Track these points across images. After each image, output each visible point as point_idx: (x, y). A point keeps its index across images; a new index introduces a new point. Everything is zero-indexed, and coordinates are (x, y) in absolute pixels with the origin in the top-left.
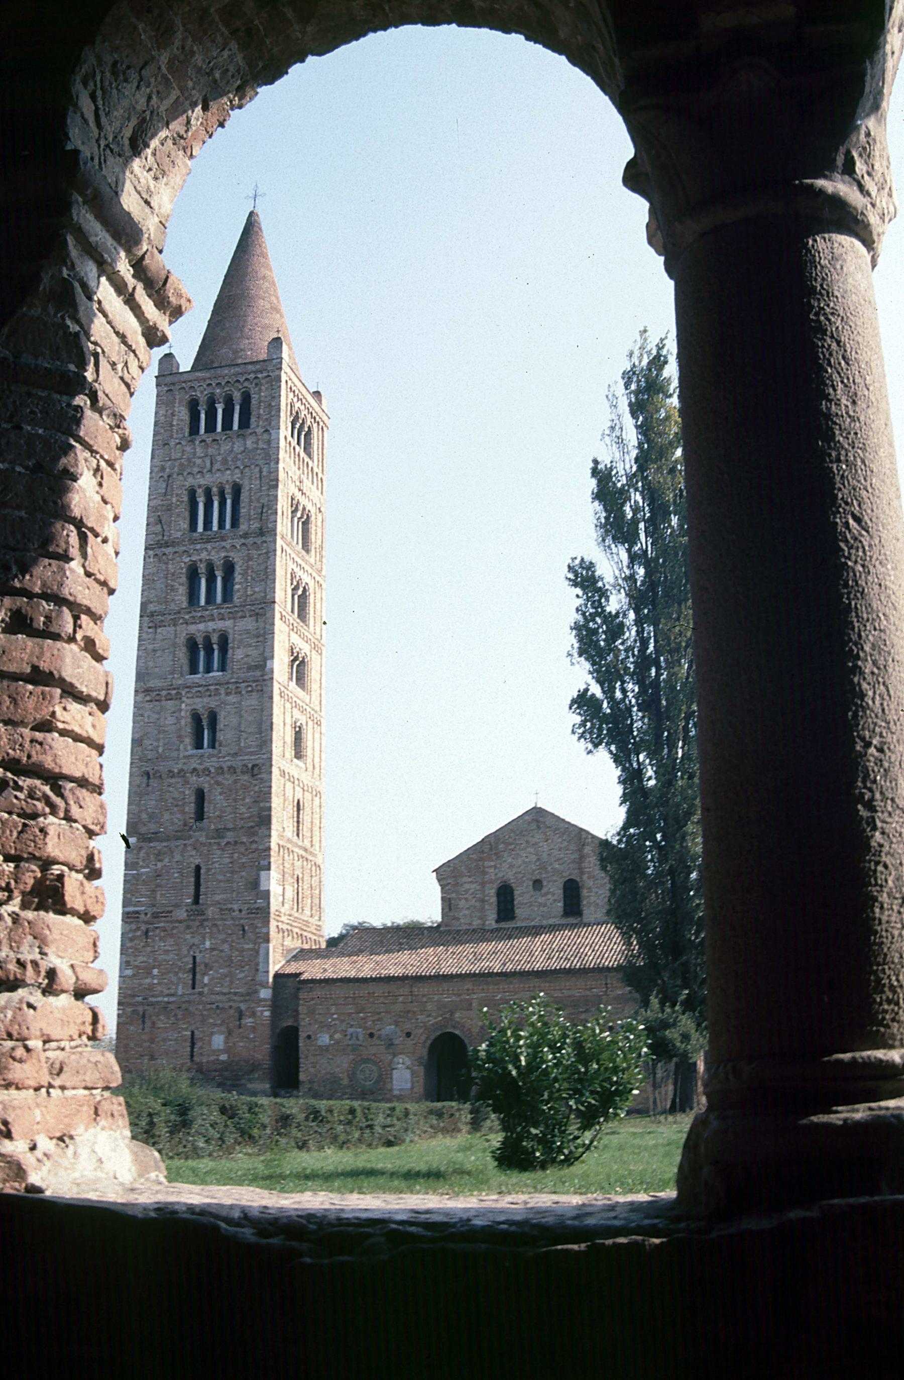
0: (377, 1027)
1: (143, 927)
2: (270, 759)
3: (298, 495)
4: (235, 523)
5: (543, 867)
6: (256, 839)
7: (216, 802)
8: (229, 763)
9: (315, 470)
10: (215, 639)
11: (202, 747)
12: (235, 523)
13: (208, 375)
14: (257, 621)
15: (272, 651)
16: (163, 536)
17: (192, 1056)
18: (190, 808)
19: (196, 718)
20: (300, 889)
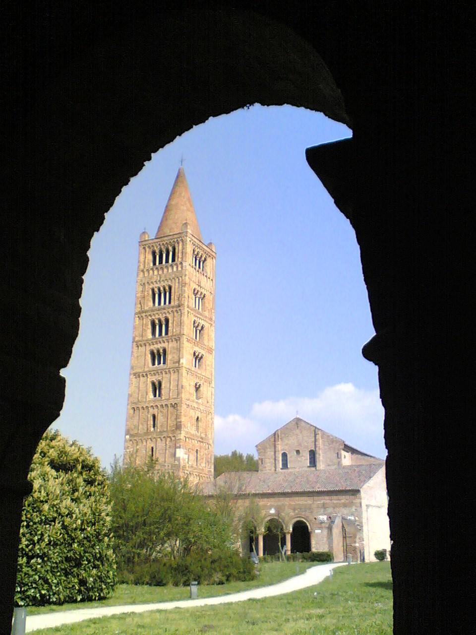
4: (170, 303)
5: (300, 445)
6: (175, 435)
7: (160, 419)
8: (166, 403)
9: (208, 276)
10: (161, 351)
12: (170, 303)
13: (159, 240)
14: (177, 342)
16: (141, 308)
19: (153, 384)
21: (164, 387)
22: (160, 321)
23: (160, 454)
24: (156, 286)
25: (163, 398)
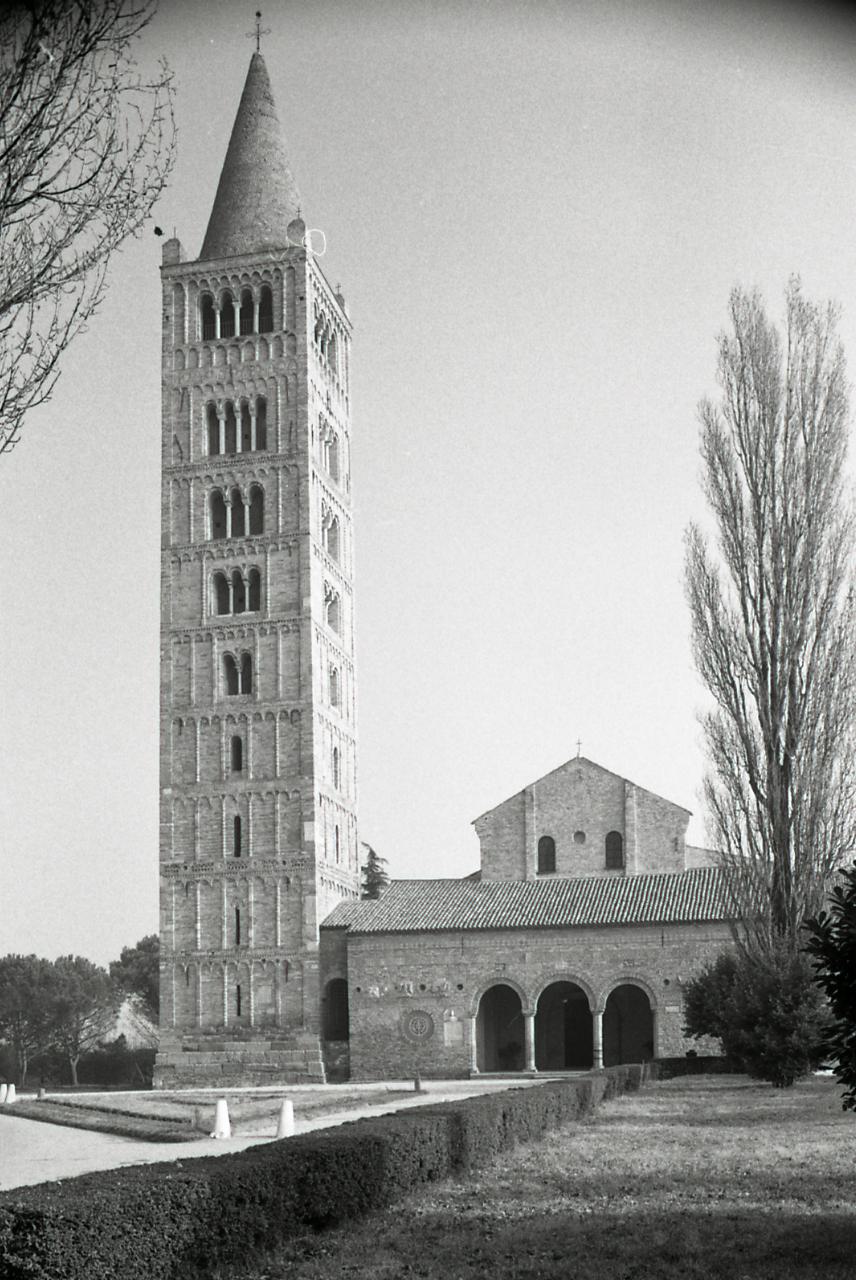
1: (184, 881)
2: (310, 705)
3: (326, 414)
6: (299, 789)
10: (246, 573)
11: (236, 693)
14: (290, 555)
15: (309, 588)
18: (227, 758)
23: (260, 834)
24: (221, 395)
25: (259, 696)
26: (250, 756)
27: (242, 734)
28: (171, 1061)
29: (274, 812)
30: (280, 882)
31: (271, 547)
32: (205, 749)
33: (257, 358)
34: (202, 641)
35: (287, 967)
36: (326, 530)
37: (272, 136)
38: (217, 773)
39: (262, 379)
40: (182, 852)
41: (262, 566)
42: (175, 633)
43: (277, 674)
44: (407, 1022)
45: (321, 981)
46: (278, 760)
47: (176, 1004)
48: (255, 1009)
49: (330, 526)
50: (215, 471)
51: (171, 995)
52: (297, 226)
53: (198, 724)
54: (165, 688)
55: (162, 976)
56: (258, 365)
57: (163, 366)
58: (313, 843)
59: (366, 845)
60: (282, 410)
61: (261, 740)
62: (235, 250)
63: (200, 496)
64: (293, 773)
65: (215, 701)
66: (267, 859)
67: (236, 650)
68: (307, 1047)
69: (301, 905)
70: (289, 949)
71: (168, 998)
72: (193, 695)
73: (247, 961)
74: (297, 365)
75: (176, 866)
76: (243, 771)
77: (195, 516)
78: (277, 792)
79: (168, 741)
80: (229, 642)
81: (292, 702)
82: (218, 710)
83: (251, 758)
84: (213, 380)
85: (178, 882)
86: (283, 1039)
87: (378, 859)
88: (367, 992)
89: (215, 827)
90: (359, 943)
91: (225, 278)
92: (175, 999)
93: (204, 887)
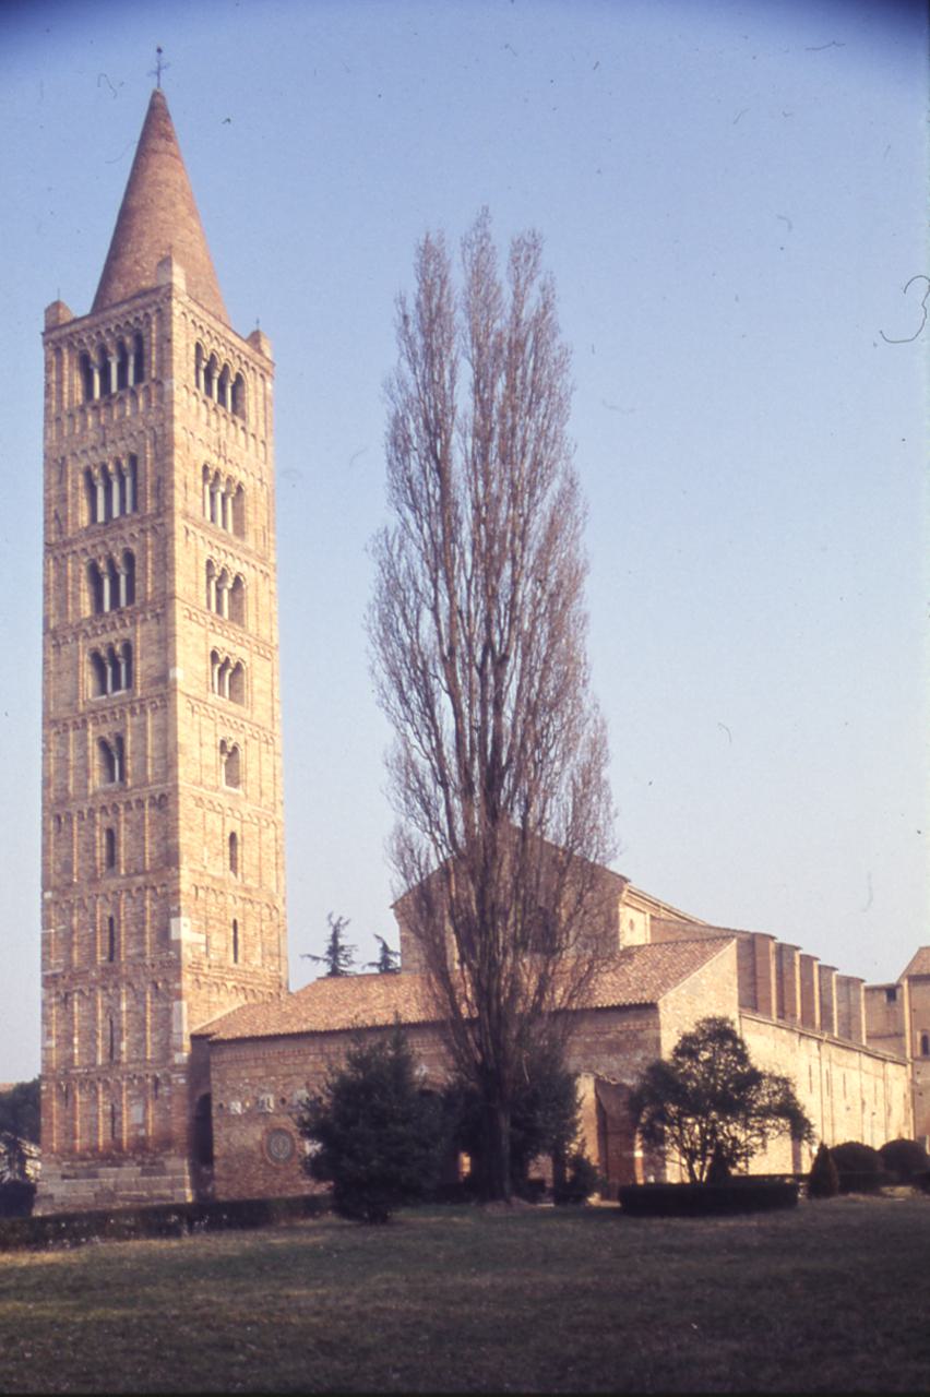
0: (288, 1092)
2: (176, 787)
6: (166, 882)
10: (118, 648)
14: (158, 623)
17: (113, 1133)
18: (101, 853)
20: (240, 936)
21: (133, 753)
22: (111, 563)
23: (131, 934)
24: (94, 458)
25: (129, 782)
26: (122, 849)
27: (115, 825)
28: (51, 1190)
29: (144, 910)
30: (149, 987)
31: (141, 617)
32: (82, 845)
33: (128, 413)
34: (78, 728)
35: (157, 1082)
36: (225, 593)
37: (164, 174)
38: (91, 871)
39: (131, 435)
40: (62, 961)
41: (132, 638)
42: (54, 722)
43: (146, 757)
44: (269, 1142)
45: (191, 1096)
46: (147, 851)
47: (57, 1128)
48: (128, 1131)
49: (230, 585)
50: (91, 542)
51: (51, 1117)
52: (165, 263)
53: (75, 819)
54: (46, 783)
55: (43, 1097)
56: (129, 421)
57: (45, 438)
58: (179, 942)
59: (378, 937)
60: (152, 465)
61: (131, 831)
62: (110, 300)
63: (77, 570)
64: (161, 865)
65: (91, 791)
66: (137, 962)
67: (109, 734)
68: (173, 1172)
69: (169, 1011)
70: (158, 1062)
71: (48, 1121)
72: (70, 788)
73: (119, 1078)
74: (164, 414)
75: (55, 976)
76: (116, 866)
77: (73, 593)
78: (146, 887)
79: (49, 839)
80: (104, 726)
81: (160, 786)
82: (93, 802)
83: (123, 853)
84: (88, 444)
85: (58, 994)
86: (152, 1164)
87: (391, 953)
88: (228, 1109)
89: (91, 930)
90: (221, 1052)
91: (99, 333)
92: (55, 1121)
93: (81, 998)
